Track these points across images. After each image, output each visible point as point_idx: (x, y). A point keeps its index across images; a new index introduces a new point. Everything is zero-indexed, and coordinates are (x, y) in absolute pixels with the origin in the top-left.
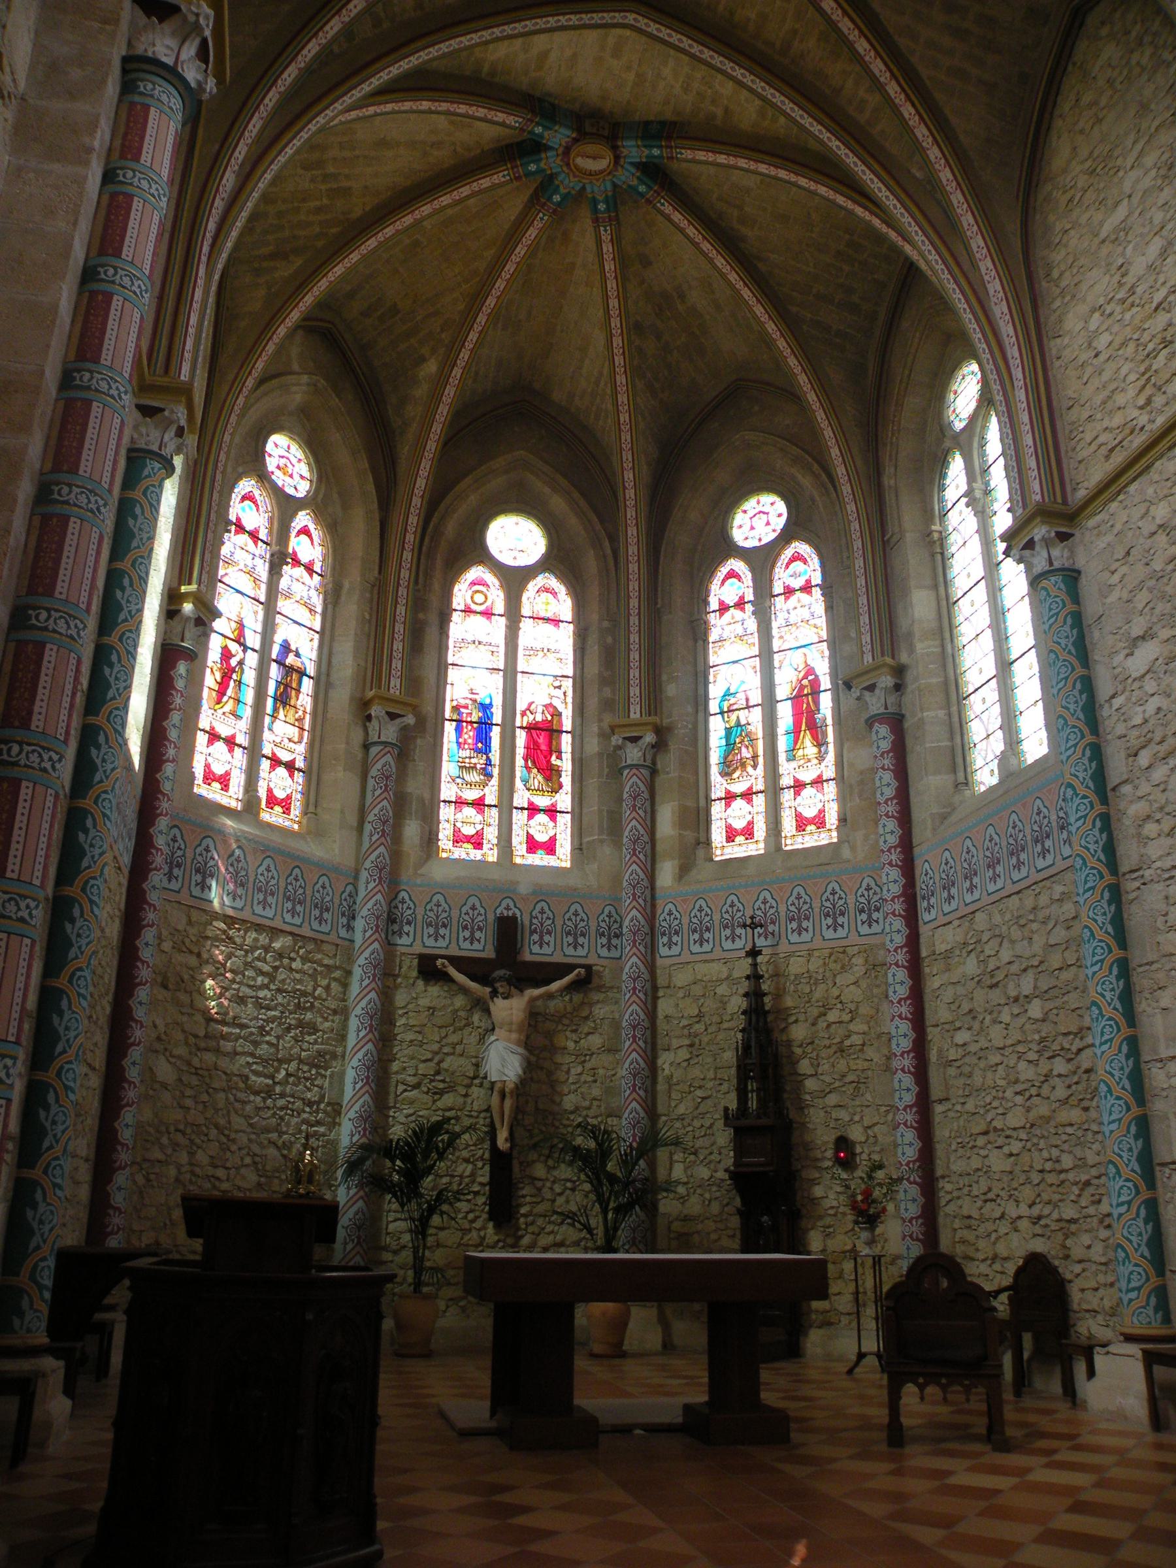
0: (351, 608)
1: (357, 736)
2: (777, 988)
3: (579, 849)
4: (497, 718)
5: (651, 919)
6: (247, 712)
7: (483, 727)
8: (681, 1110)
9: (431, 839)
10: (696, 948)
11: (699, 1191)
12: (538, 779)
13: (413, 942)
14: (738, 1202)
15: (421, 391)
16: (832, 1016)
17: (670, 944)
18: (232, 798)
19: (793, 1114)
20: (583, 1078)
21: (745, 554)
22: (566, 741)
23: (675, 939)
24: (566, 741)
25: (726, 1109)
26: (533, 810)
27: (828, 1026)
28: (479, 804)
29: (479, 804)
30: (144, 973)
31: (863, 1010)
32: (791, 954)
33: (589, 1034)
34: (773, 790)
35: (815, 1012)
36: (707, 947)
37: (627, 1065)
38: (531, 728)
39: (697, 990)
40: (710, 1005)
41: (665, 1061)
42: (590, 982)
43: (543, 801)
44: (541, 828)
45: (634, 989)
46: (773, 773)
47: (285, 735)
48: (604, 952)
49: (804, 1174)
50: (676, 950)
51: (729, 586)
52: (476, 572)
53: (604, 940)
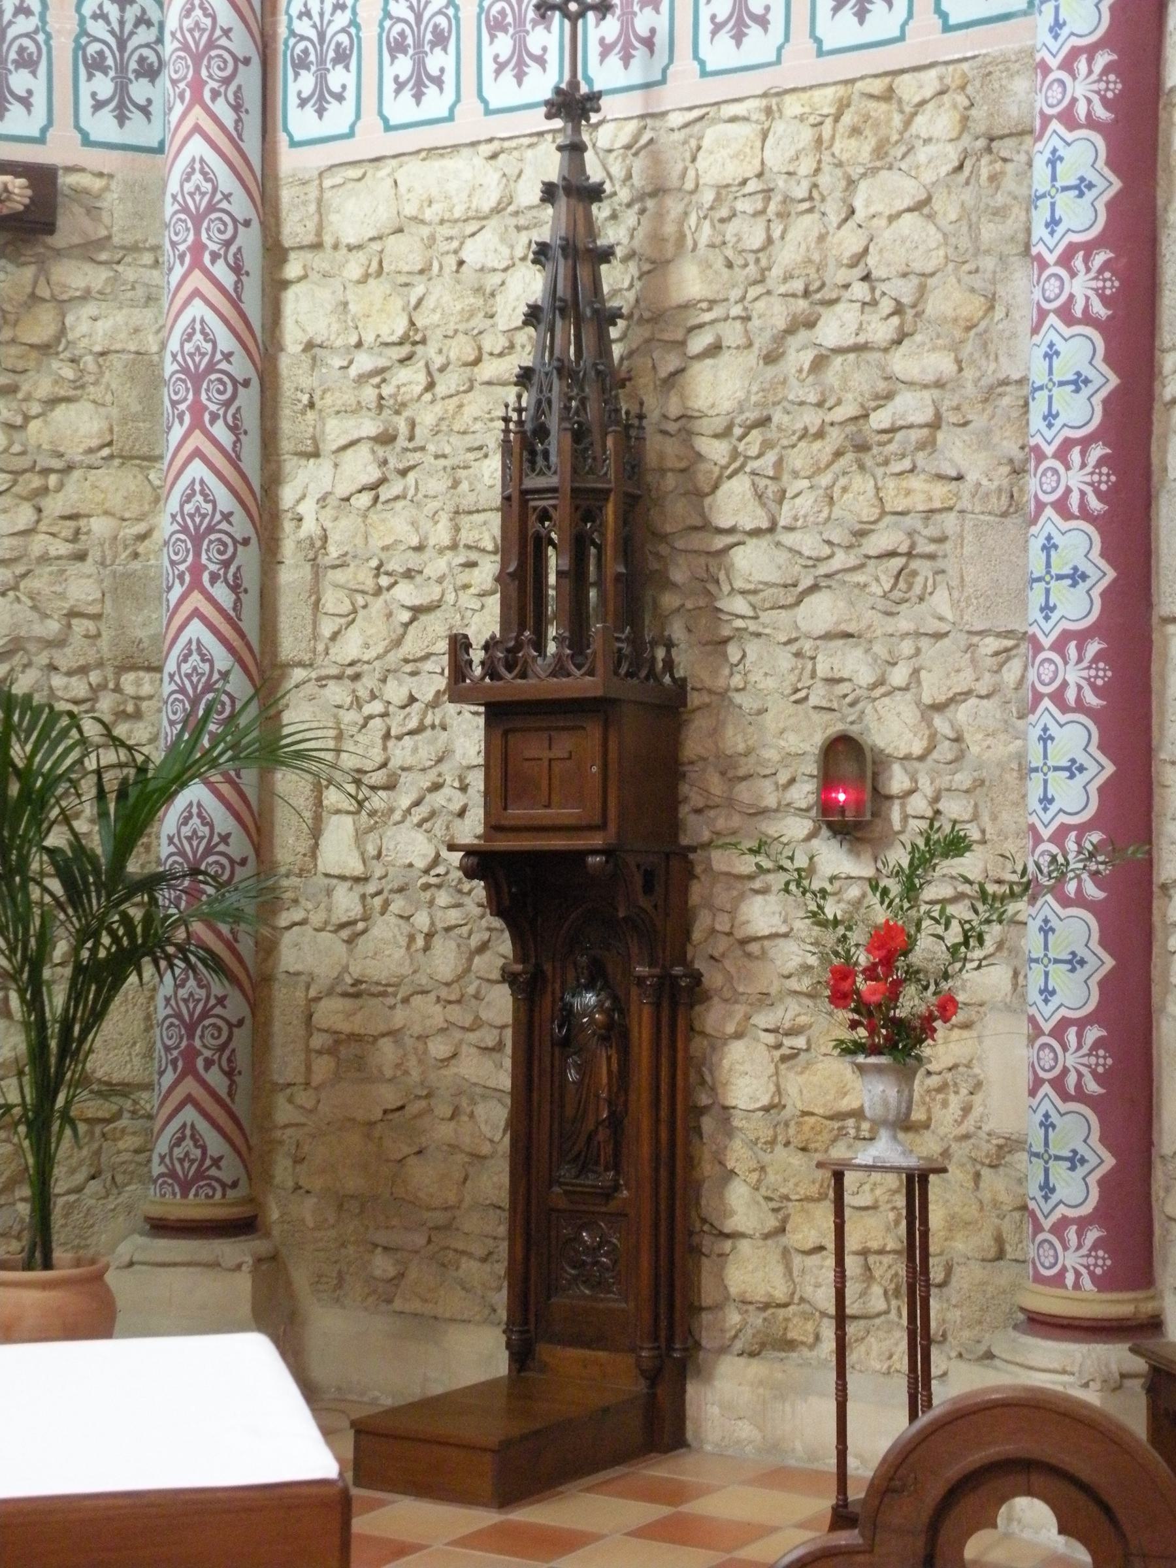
2: (657, 238)
8: (350, 647)
10: (401, 108)
11: (398, 905)
14: (505, 946)
16: (834, 329)
17: (321, 98)
19: (687, 661)
20: (38, 544)
23: (337, 78)
25: (459, 644)
27: (819, 363)
31: (947, 300)
32: (704, 115)
33: (53, 402)
35: (774, 314)
36: (435, 103)
37: (173, 504)
39: (404, 253)
40: (444, 302)
41: (304, 488)
42: (49, 228)
45: (198, 248)
48: (103, 126)
49: (720, 860)
50: (338, 117)
53: (104, 86)
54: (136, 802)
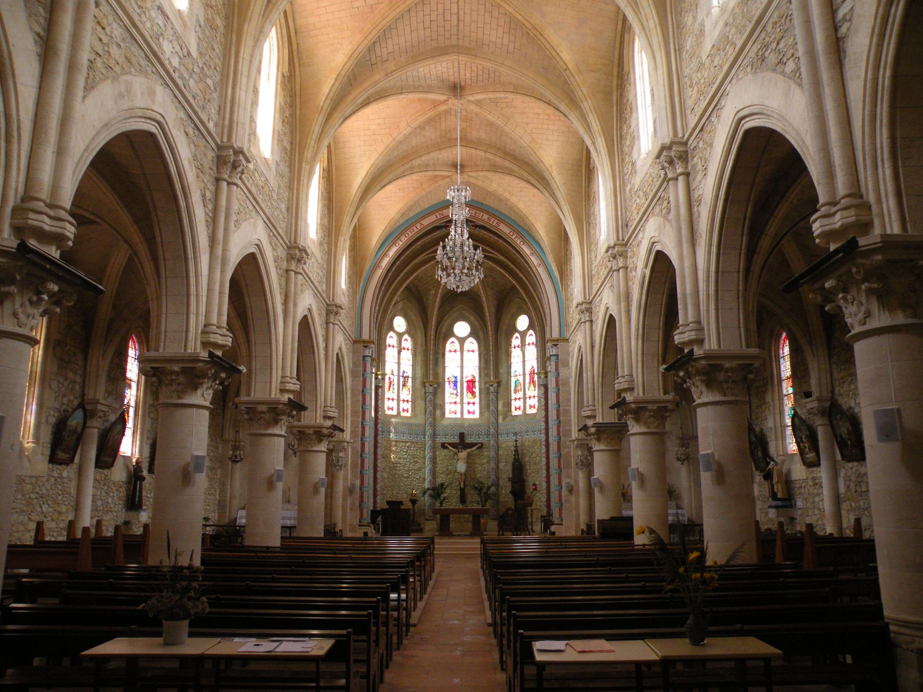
0: (419, 358)
1: (423, 390)
3: (481, 413)
4: (459, 380)
5: (497, 432)
6: (396, 391)
7: (455, 383)
9: (443, 413)
12: (470, 395)
13: (440, 440)
15: (431, 298)
18: (394, 412)
21: (519, 332)
22: (477, 384)
24: (477, 384)
26: (469, 403)
28: (455, 403)
29: (455, 403)
30: (379, 457)
34: (525, 398)
38: (468, 382)
41: (501, 465)
43: (471, 401)
44: (471, 408)
46: (525, 394)
47: (406, 394)
51: (516, 341)
52: (452, 339)
54: (489, 488)
